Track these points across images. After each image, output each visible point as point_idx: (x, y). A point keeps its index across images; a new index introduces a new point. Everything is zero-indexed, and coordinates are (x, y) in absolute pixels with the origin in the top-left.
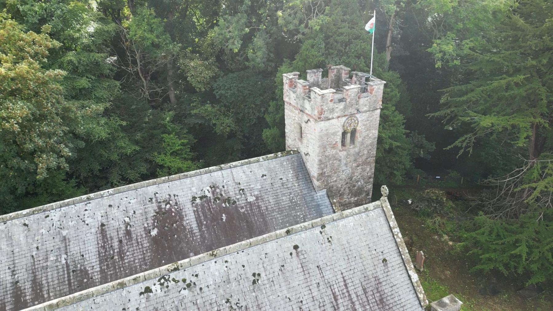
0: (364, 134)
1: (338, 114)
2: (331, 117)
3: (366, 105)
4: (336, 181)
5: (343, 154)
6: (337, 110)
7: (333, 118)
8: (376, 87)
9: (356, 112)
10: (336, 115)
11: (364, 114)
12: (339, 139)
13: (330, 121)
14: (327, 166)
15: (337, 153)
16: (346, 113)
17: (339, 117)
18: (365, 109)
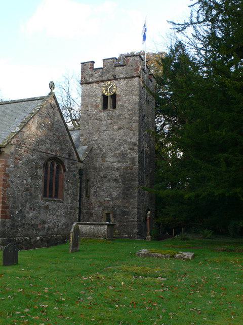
0: (125, 98)
1: (97, 79)
2: (90, 81)
3: (122, 73)
4: (97, 140)
5: (103, 114)
6: (96, 75)
7: (92, 83)
8: (131, 58)
9: (113, 78)
10: (95, 80)
11: (122, 80)
12: (99, 100)
13: (91, 85)
14: (88, 123)
15: (97, 114)
16: (104, 78)
17: (97, 82)
18: (122, 76)
